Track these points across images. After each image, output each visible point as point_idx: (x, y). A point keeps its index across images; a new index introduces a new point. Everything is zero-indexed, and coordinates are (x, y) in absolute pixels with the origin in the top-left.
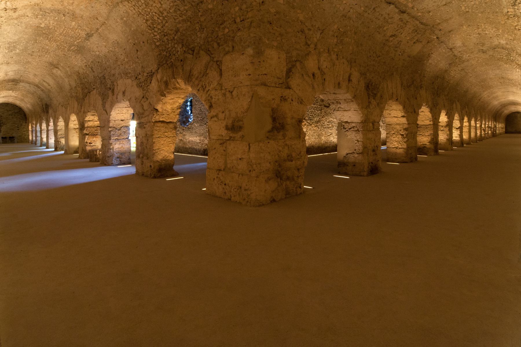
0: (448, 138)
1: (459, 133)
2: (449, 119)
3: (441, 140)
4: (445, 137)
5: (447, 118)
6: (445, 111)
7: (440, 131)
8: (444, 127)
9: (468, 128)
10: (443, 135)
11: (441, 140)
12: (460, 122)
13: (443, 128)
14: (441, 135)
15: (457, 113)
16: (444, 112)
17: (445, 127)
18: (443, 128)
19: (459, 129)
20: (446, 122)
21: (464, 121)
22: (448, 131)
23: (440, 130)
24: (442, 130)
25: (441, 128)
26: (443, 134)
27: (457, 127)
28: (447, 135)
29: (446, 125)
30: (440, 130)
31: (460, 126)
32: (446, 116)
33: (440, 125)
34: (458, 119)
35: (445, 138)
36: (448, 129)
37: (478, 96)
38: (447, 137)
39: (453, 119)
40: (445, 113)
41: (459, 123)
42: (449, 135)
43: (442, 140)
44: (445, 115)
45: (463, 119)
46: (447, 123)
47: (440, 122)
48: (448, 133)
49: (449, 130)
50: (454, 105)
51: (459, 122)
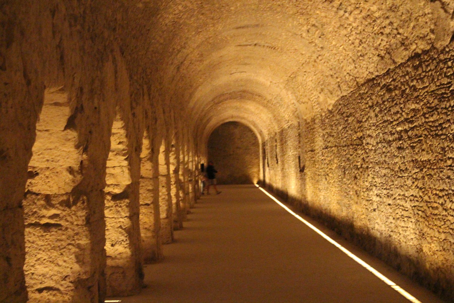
0: (84, 277)
1: (126, 222)
2: (85, 150)
3: (45, 294)
4: (68, 271)
5: (77, 147)
6: (62, 98)
7: (38, 231)
8: (61, 203)
9: (150, 188)
10: (55, 254)
11: (40, 291)
12: (130, 164)
13: (53, 211)
14: (43, 255)
15: (118, 117)
16: (57, 104)
17: (67, 204)
18: (53, 211)
19: (127, 201)
20: (71, 170)
21: (142, 155)
22: (83, 231)
23: (36, 225)
24: (47, 227)
25: (44, 212)
26: (54, 248)
27: (117, 191)
28: (79, 260)
29: (69, 189)
30: (36, 225)
31: (129, 183)
32: (73, 134)
33: (34, 189)
34: (121, 147)
35: (65, 278)
36: (82, 214)
37: (179, 51)
38: (76, 267)
39: (107, 148)
40: (67, 111)
41: (126, 171)
42: (88, 252)
43: (48, 289)
44: (66, 128)
45: (138, 149)
46: (79, 178)
47: (33, 175)
48: (84, 241)
49: (88, 221)
50: (109, 67)
51: (125, 163)
